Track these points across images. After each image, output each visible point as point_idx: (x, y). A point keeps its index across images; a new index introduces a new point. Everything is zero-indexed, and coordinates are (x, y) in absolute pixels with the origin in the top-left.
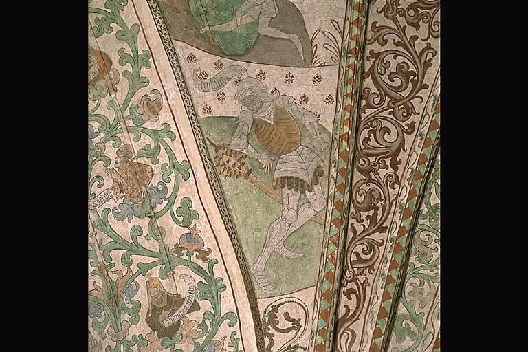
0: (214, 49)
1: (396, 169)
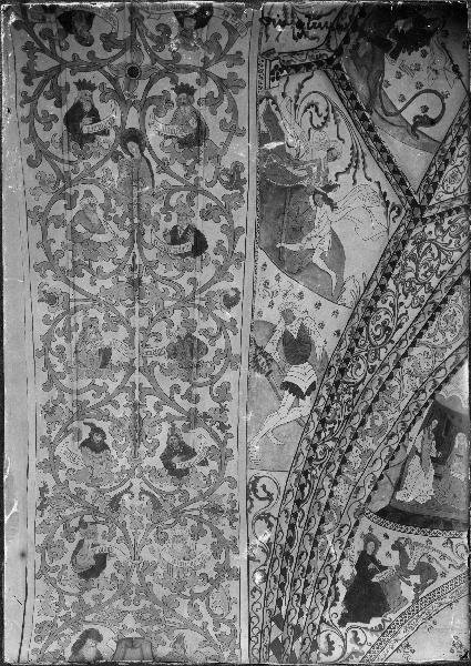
0: (280, 263)
1: (354, 396)
